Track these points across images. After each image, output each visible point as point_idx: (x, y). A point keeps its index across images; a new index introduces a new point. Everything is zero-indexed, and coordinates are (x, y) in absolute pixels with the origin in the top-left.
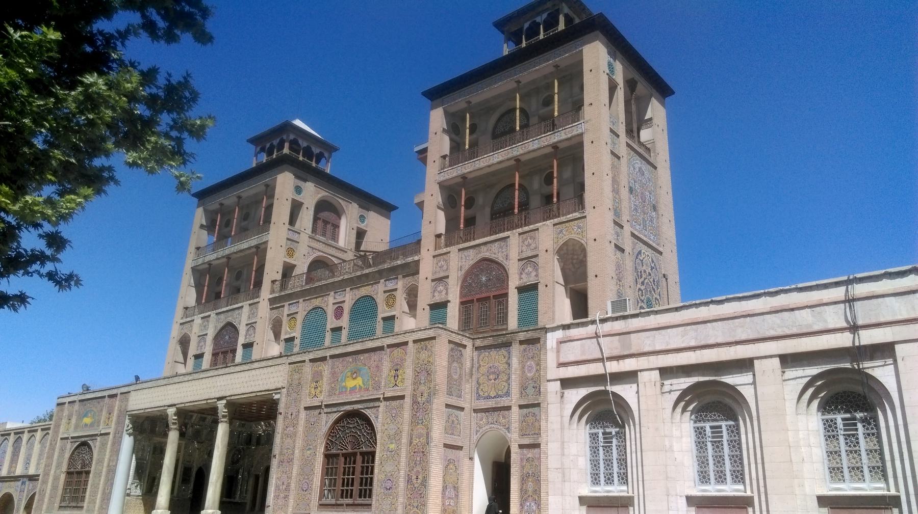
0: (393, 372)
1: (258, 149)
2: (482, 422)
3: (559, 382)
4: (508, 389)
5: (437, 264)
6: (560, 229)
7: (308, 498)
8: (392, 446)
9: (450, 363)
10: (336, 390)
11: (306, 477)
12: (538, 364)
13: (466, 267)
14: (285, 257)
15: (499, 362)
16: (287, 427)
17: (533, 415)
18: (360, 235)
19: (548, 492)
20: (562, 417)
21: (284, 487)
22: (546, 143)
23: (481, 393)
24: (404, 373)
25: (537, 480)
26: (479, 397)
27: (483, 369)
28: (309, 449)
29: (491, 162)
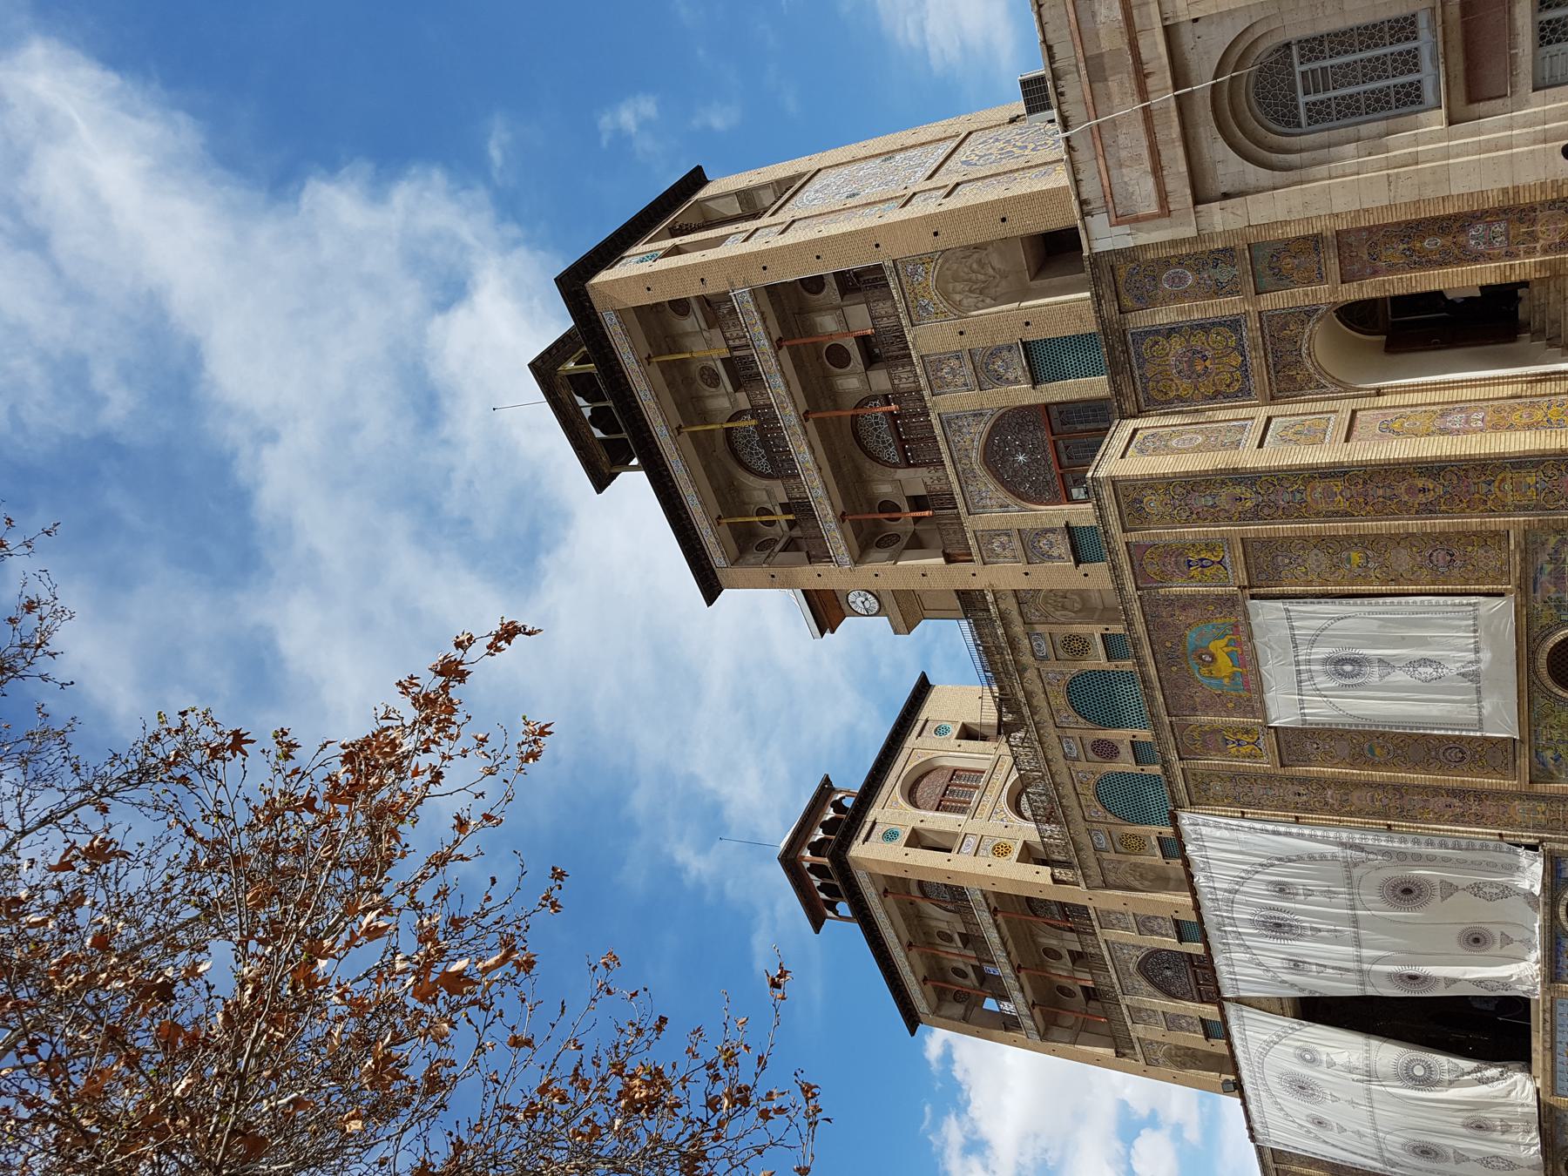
0: (1194, 571)
1: (830, 914)
2: (1298, 377)
3: (1200, 207)
7: (1479, 746)
9: (1173, 451)
10: (1240, 696)
11: (1433, 753)
12: (1166, 263)
13: (1002, 495)
16: (1326, 803)
17: (1275, 259)
18: (968, 733)
21: (1456, 802)
22: (773, 360)
24: (1194, 545)
28: (1372, 751)
29: (810, 465)
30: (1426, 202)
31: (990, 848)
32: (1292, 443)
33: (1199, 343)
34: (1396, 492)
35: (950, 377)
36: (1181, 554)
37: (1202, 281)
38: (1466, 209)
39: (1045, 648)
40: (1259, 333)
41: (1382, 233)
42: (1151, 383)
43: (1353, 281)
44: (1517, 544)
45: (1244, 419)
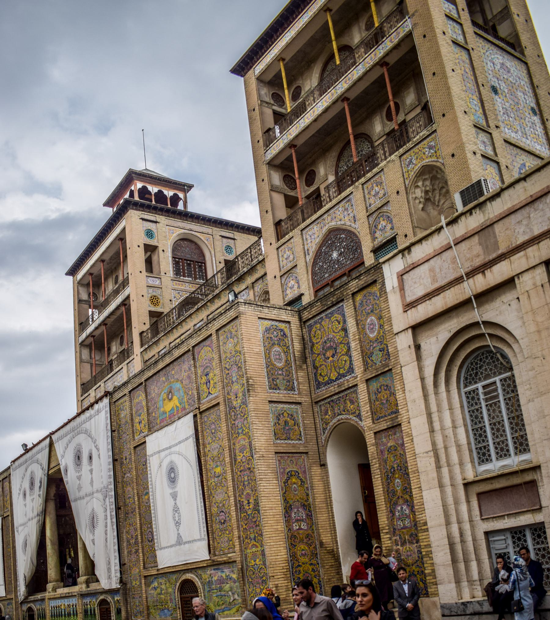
0: (204, 379)
2: (327, 416)
4: (350, 364)
5: (282, 256)
8: (218, 470)
15: (334, 332)
17: (385, 388)
19: (420, 487)
20: (422, 379)
23: (321, 380)
25: (405, 474)
26: (319, 385)
27: (317, 348)
30: (418, 477)
32: (276, 421)
33: (340, 351)
34: (247, 487)
36: (211, 369)
37: (372, 344)
38: (415, 502)
40: (347, 387)
41: (402, 452)
42: (319, 325)
44: (230, 558)
45: (299, 389)
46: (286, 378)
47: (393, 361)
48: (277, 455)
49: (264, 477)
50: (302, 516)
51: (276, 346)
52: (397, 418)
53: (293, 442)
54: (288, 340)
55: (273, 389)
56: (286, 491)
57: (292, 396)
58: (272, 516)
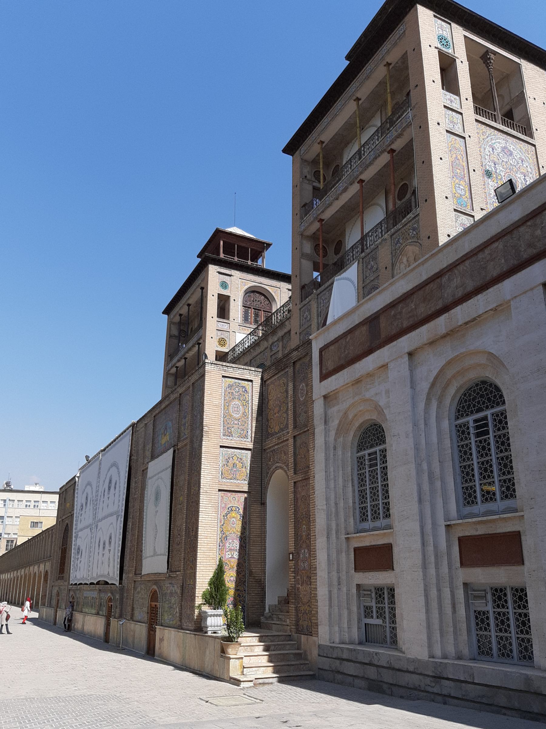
2: (270, 463)
6: (397, 239)
14: (217, 347)
15: (281, 392)
29: (338, 192)
31: (222, 337)
32: (225, 463)
35: (369, 267)
39: (275, 349)
43: (294, 488)
46: (242, 427)
47: (310, 423)
48: (220, 492)
49: (205, 509)
50: (236, 547)
51: (236, 400)
52: (308, 472)
53: (239, 481)
54: (248, 396)
55: (227, 436)
56: (224, 523)
57: (244, 443)
58: (206, 544)
